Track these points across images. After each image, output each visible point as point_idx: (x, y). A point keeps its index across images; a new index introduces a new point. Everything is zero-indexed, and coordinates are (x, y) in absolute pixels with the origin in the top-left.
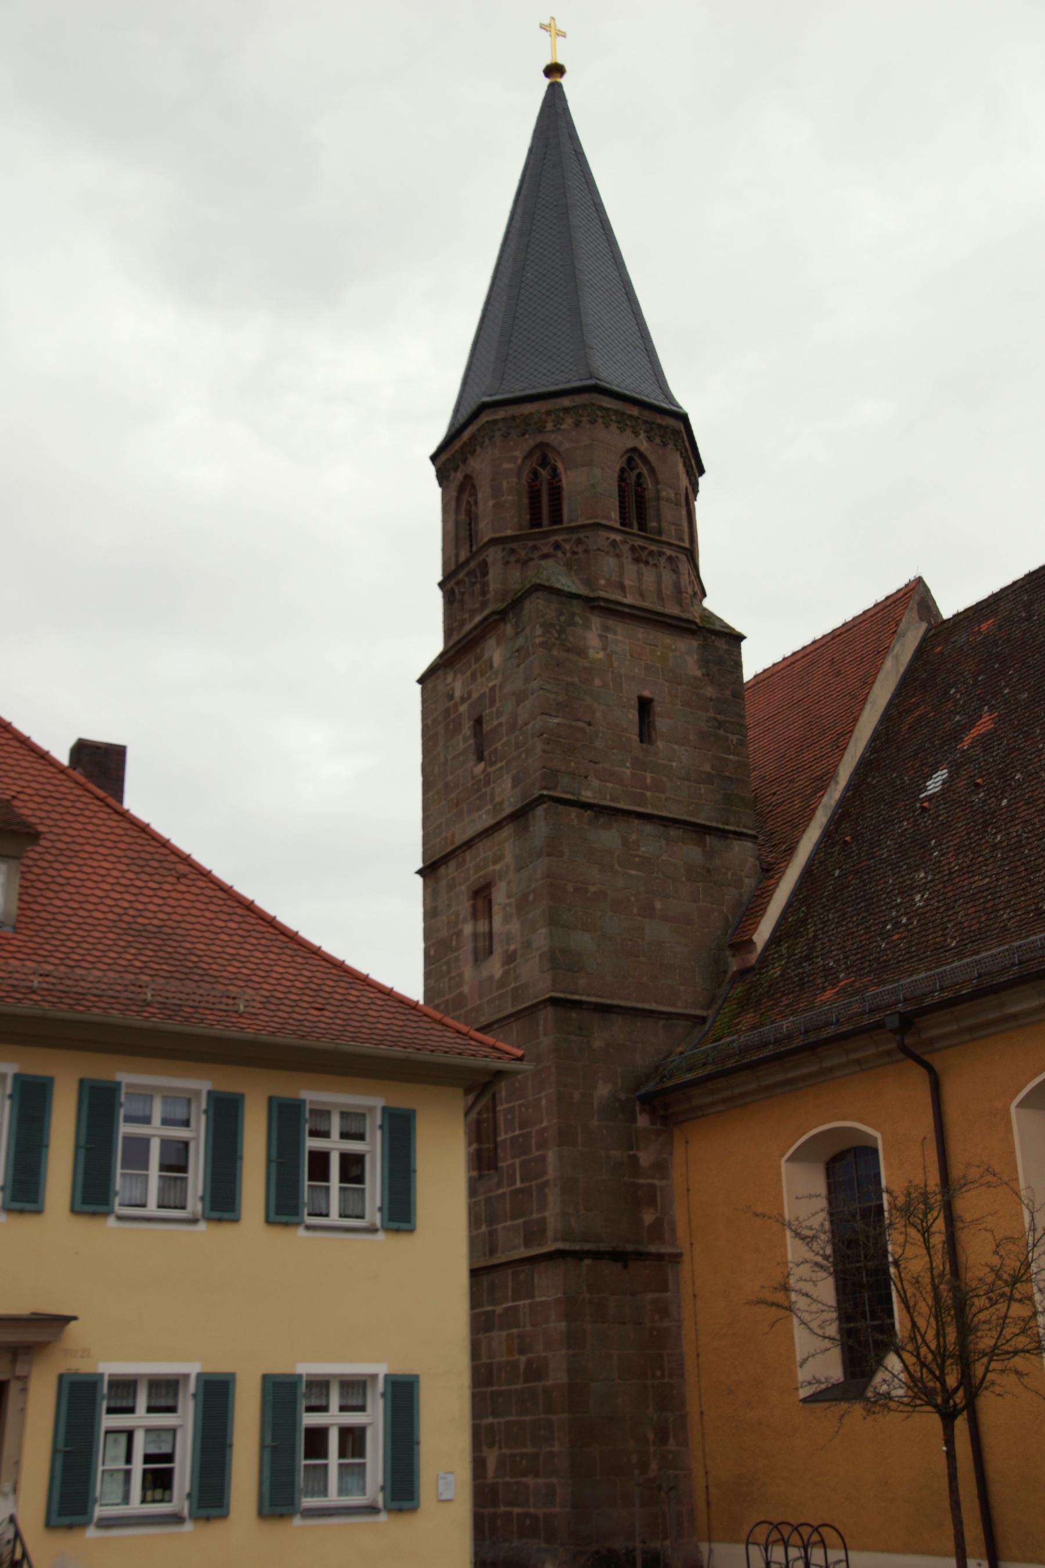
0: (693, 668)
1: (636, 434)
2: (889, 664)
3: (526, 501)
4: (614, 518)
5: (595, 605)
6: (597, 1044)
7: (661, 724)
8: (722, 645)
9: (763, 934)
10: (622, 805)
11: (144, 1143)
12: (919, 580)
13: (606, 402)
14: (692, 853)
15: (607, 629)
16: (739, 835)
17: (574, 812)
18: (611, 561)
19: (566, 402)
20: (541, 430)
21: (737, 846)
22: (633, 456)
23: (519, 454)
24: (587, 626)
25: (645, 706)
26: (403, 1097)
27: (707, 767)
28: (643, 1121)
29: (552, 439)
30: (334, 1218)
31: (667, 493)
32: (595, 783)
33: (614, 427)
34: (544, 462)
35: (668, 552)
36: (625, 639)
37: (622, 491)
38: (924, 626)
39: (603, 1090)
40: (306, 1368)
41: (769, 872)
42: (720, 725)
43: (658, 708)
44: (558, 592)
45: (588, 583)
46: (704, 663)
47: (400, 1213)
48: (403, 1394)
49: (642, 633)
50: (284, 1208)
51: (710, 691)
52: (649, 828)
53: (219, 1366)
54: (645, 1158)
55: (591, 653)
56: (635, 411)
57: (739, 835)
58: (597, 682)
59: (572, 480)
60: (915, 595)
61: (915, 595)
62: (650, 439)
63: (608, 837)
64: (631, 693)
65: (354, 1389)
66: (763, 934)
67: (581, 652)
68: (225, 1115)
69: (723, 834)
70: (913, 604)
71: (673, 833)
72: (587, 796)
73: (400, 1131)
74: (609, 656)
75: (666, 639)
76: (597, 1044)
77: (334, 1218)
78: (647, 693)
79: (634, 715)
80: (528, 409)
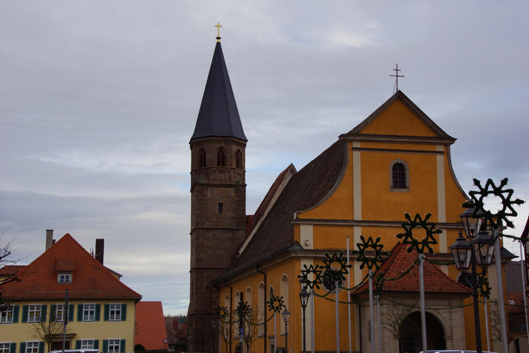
0: (233, 194)
1: (222, 143)
2: (281, 186)
3: (200, 160)
4: (215, 164)
5: (208, 185)
6: (205, 275)
7: (224, 208)
8: (241, 187)
9: (241, 252)
10: (214, 227)
11: (88, 311)
12: (292, 164)
13: (214, 138)
14: (230, 235)
15: (212, 190)
16: (241, 229)
17: (202, 230)
18: (214, 174)
19: (206, 139)
20: (202, 144)
21: (241, 231)
22: (221, 148)
23: (198, 150)
24: (207, 190)
25: (221, 205)
26: (124, 303)
27: (235, 216)
28: (214, 289)
29: (204, 147)
30: (115, 319)
31: (229, 155)
32: (207, 223)
33: (216, 143)
34: (203, 151)
35: (228, 169)
36: (216, 191)
37: (219, 157)
38: (292, 175)
39: (205, 284)
40: (109, 339)
41: (247, 237)
42: (239, 206)
43: (223, 205)
44: (201, 184)
45: (209, 180)
46: (236, 192)
47: (124, 318)
48: (123, 342)
49: (221, 189)
50: (106, 318)
51: (237, 199)
52: (219, 231)
53: (97, 339)
54: (214, 296)
55: (208, 196)
56: (221, 139)
57: (241, 229)
58: (209, 202)
59: (208, 156)
60: (291, 168)
61: (291, 168)
62: (225, 144)
63: (210, 234)
64: (217, 203)
65: (117, 341)
66: (241, 252)
67: (206, 196)
68: (98, 307)
69: (237, 230)
70: (289, 171)
71: (225, 231)
72: (205, 226)
73: (124, 308)
74: (212, 196)
75: (227, 189)
76: (205, 275)
77: (115, 319)
78: (221, 202)
79: (218, 207)
80: (199, 140)
